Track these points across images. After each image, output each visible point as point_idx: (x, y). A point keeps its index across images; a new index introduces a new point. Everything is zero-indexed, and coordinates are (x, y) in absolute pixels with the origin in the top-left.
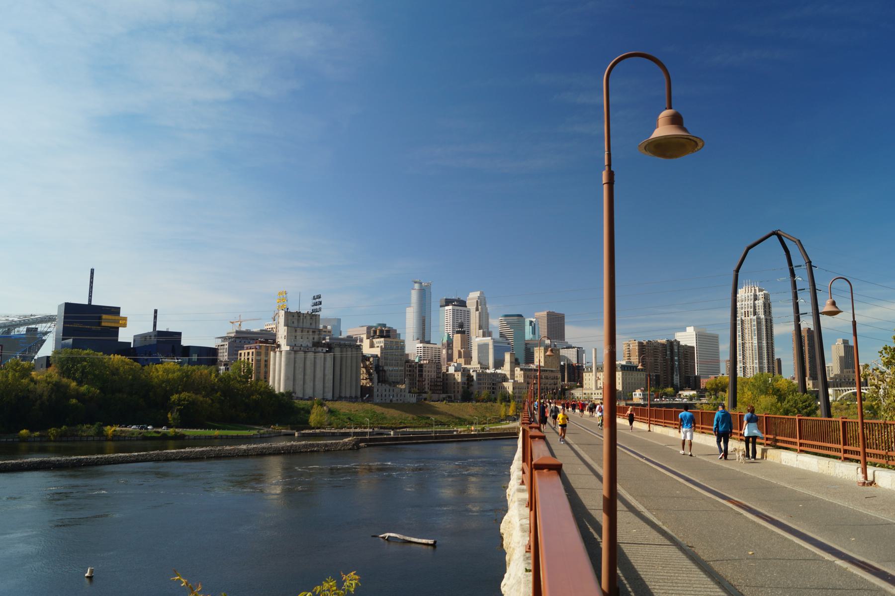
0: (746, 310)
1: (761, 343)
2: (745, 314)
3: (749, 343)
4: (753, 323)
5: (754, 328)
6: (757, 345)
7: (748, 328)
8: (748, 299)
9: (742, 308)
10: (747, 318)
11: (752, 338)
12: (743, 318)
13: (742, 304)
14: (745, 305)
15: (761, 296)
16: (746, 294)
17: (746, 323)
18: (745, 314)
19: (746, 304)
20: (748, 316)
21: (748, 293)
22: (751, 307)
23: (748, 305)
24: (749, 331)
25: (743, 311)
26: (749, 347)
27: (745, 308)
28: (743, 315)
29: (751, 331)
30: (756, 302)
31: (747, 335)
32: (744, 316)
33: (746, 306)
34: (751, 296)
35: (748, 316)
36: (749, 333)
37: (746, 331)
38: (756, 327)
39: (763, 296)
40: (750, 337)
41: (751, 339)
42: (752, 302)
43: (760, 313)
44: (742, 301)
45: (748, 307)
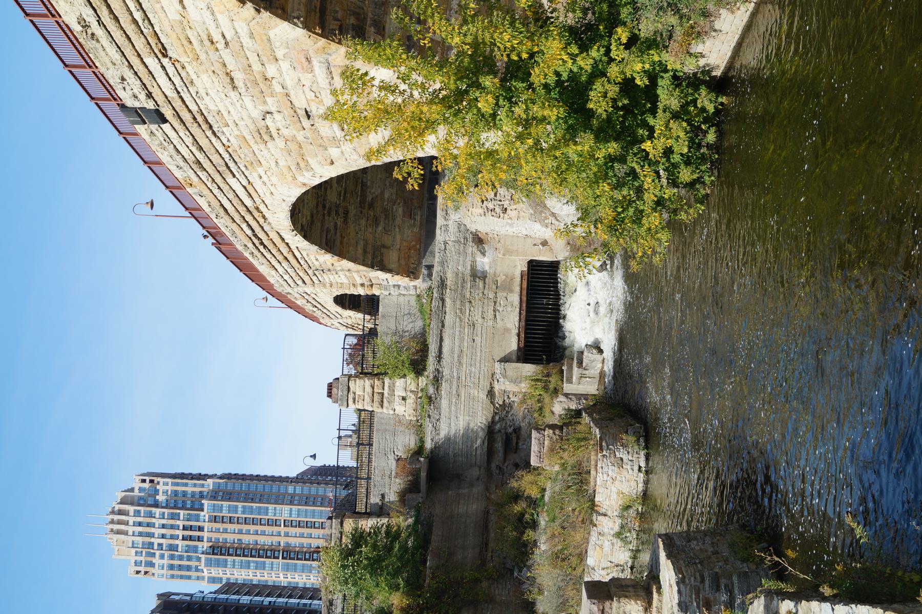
0: (180, 533)
1: (293, 496)
2: (191, 538)
3: (287, 535)
4: (225, 513)
5: (240, 509)
6: (295, 508)
7: (240, 532)
8: (148, 525)
9: (173, 548)
10: (205, 535)
11: (276, 523)
12: (205, 545)
13: (160, 545)
14: (163, 536)
15: (147, 485)
16: (131, 530)
17: (222, 537)
18: (191, 538)
19: (163, 531)
20: (201, 529)
21: (127, 523)
22: (173, 517)
23: (164, 526)
24: (248, 532)
25: (180, 543)
26: (302, 536)
27: (172, 537)
28: (196, 547)
29: (254, 522)
30: (161, 498)
31: (262, 540)
32: (199, 544)
33: (168, 532)
34: (137, 514)
35: (201, 529)
36: (256, 533)
37: (247, 539)
38: (240, 505)
39: (148, 479)
40: (268, 529)
41: (275, 529)
42: (157, 511)
43: (197, 490)
44: (151, 545)
45: (172, 527)
